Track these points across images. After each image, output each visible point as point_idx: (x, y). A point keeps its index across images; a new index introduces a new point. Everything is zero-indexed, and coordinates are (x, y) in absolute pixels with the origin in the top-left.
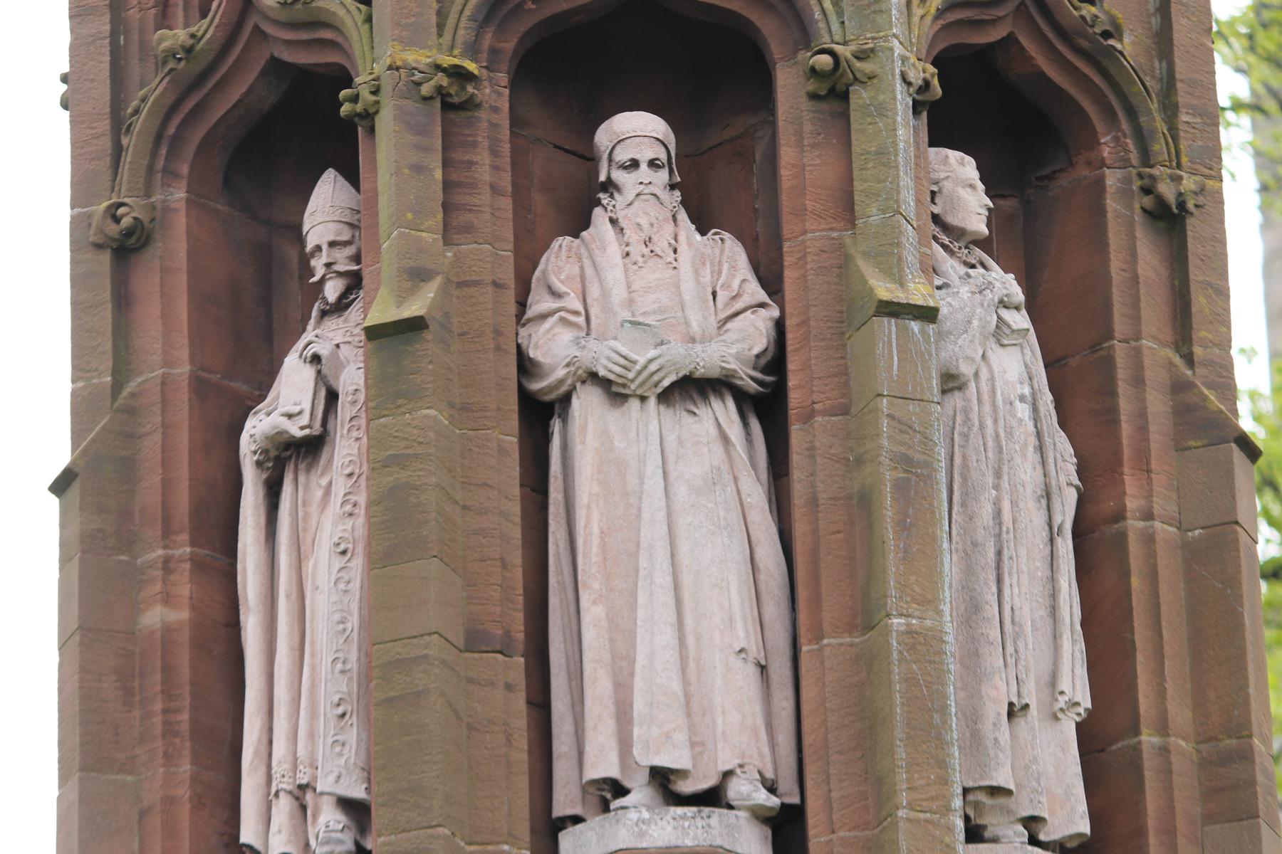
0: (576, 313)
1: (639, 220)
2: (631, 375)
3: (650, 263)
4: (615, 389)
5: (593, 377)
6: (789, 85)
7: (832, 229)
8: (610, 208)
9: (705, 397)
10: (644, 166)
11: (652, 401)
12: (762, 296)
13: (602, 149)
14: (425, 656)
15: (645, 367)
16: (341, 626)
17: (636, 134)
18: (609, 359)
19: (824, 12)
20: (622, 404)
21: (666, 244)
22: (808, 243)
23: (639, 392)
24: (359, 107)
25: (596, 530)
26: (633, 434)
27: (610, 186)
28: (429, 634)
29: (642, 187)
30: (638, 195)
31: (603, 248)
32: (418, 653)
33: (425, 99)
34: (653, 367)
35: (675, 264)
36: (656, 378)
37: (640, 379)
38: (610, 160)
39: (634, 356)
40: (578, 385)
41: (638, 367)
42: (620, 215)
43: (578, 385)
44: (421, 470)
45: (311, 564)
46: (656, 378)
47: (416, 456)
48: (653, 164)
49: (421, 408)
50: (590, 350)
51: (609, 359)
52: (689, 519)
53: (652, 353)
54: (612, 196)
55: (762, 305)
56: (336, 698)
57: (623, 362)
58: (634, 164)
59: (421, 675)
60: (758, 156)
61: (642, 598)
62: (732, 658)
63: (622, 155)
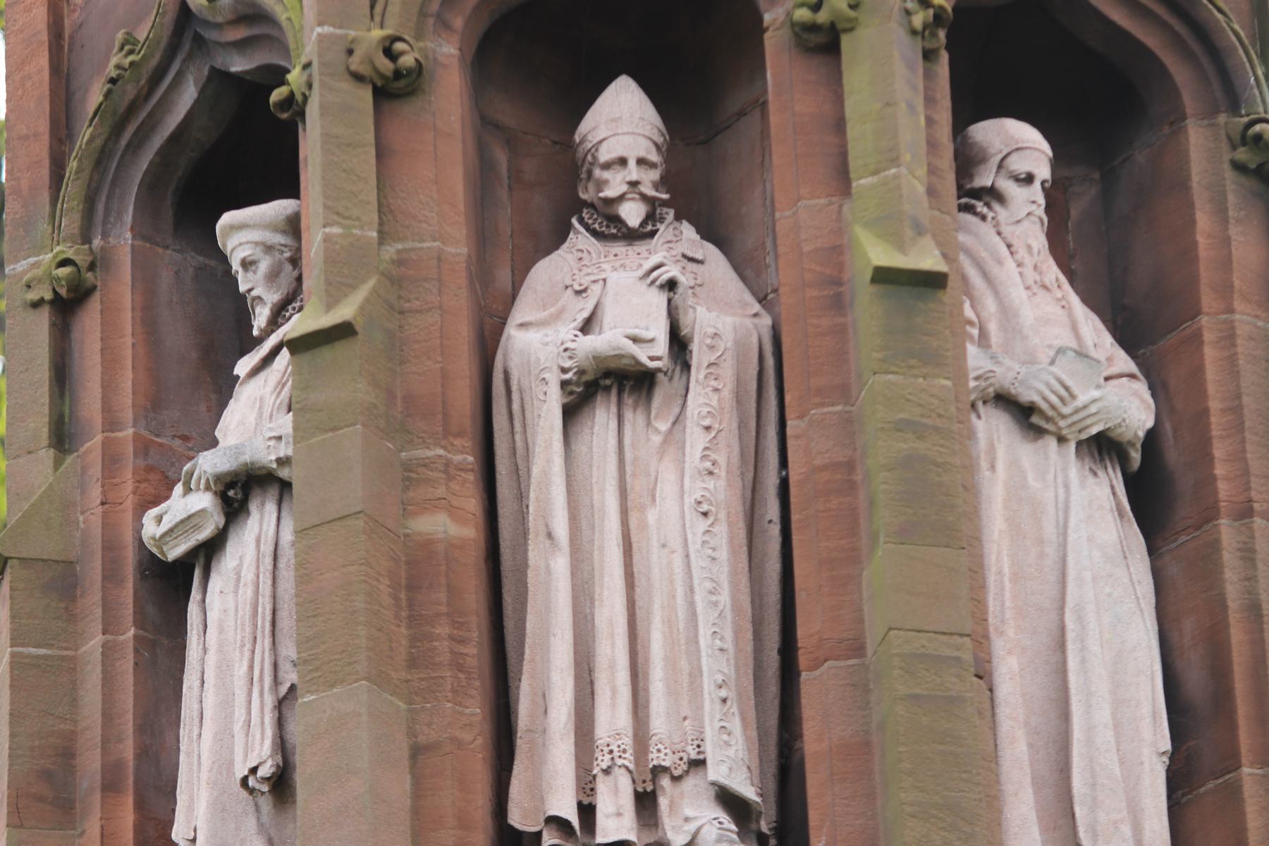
0: (971, 323)
1: (1030, 241)
2: (1066, 410)
3: (1041, 292)
4: (1035, 419)
5: (1004, 400)
6: (1202, 149)
7: (1257, 317)
8: (989, 219)
9: (1102, 460)
10: (1037, 184)
11: (1072, 446)
12: (1132, 367)
13: (992, 151)
14: (957, 659)
15: (1085, 407)
16: (714, 598)
17: (1019, 144)
18: (1048, 385)
19: (1257, 79)
20: (1036, 439)
21: (1053, 277)
22: (1237, 324)
23: (1064, 432)
24: (822, 17)
25: (1006, 570)
26: (1050, 477)
27: (993, 195)
28: (962, 635)
29: (1034, 207)
30: (1029, 214)
31: (1000, 262)
32: (947, 652)
33: (914, 32)
34: (1093, 409)
35: (1064, 303)
36: (1089, 422)
37: (1076, 418)
38: (1000, 166)
39: (1076, 390)
40: (980, 404)
41: (1080, 402)
42: (1006, 230)
43: (980, 404)
44: (942, 446)
45: (652, 516)
46: (1089, 422)
47: (937, 429)
48: (1043, 183)
49: (938, 376)
50: (1009, 369)
51: (1048, 385)
52: (1107, 590)
53: (1096, 394)
54: (987, 205)
55: (1132, 376)
56: (720, 678)
57: (1063, 392)
58: (1029, 179)
59: (954, 679)
60: (1075, 211)
61: (1072, 664)
62: (1155, 759)
63: (1019, 164)
